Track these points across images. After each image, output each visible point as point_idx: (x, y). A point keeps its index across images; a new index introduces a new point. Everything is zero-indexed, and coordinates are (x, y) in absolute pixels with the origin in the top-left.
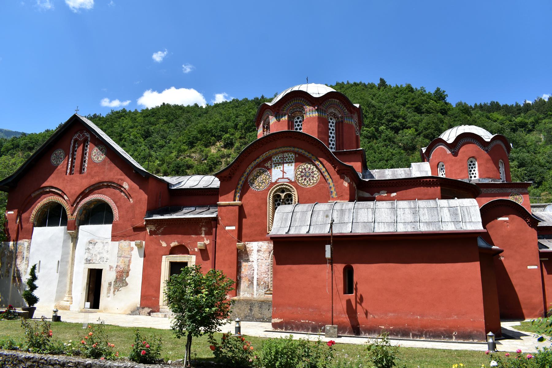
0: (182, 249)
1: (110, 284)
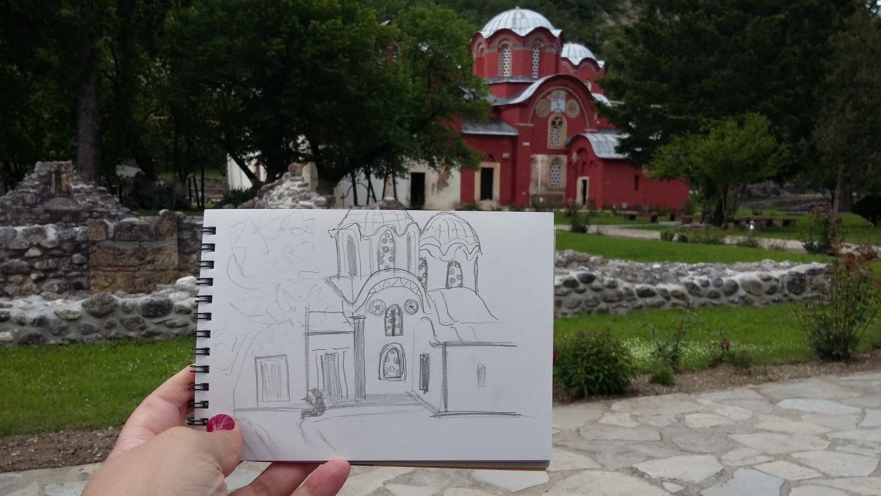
0: (492, 159)
1: (433, 185)
